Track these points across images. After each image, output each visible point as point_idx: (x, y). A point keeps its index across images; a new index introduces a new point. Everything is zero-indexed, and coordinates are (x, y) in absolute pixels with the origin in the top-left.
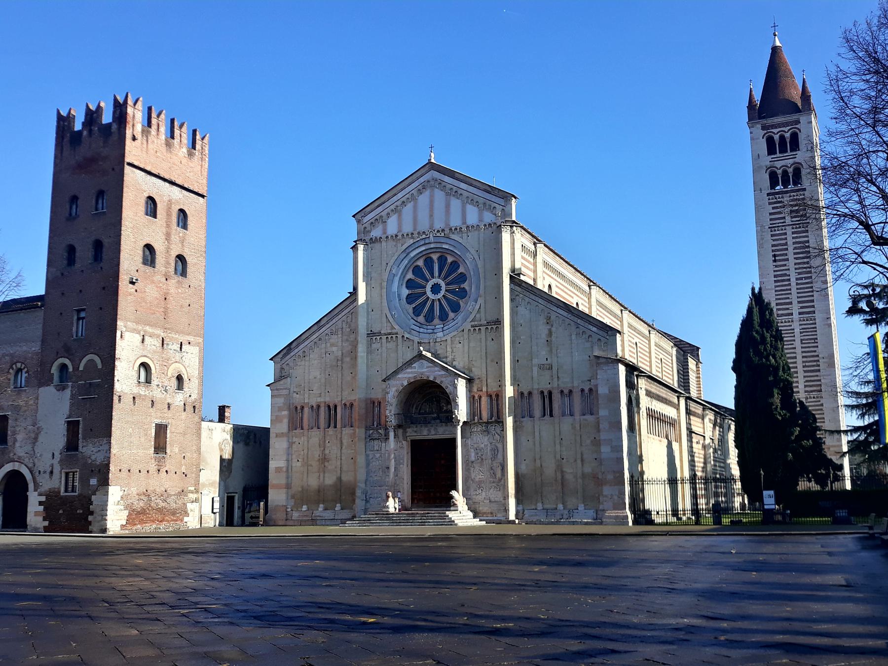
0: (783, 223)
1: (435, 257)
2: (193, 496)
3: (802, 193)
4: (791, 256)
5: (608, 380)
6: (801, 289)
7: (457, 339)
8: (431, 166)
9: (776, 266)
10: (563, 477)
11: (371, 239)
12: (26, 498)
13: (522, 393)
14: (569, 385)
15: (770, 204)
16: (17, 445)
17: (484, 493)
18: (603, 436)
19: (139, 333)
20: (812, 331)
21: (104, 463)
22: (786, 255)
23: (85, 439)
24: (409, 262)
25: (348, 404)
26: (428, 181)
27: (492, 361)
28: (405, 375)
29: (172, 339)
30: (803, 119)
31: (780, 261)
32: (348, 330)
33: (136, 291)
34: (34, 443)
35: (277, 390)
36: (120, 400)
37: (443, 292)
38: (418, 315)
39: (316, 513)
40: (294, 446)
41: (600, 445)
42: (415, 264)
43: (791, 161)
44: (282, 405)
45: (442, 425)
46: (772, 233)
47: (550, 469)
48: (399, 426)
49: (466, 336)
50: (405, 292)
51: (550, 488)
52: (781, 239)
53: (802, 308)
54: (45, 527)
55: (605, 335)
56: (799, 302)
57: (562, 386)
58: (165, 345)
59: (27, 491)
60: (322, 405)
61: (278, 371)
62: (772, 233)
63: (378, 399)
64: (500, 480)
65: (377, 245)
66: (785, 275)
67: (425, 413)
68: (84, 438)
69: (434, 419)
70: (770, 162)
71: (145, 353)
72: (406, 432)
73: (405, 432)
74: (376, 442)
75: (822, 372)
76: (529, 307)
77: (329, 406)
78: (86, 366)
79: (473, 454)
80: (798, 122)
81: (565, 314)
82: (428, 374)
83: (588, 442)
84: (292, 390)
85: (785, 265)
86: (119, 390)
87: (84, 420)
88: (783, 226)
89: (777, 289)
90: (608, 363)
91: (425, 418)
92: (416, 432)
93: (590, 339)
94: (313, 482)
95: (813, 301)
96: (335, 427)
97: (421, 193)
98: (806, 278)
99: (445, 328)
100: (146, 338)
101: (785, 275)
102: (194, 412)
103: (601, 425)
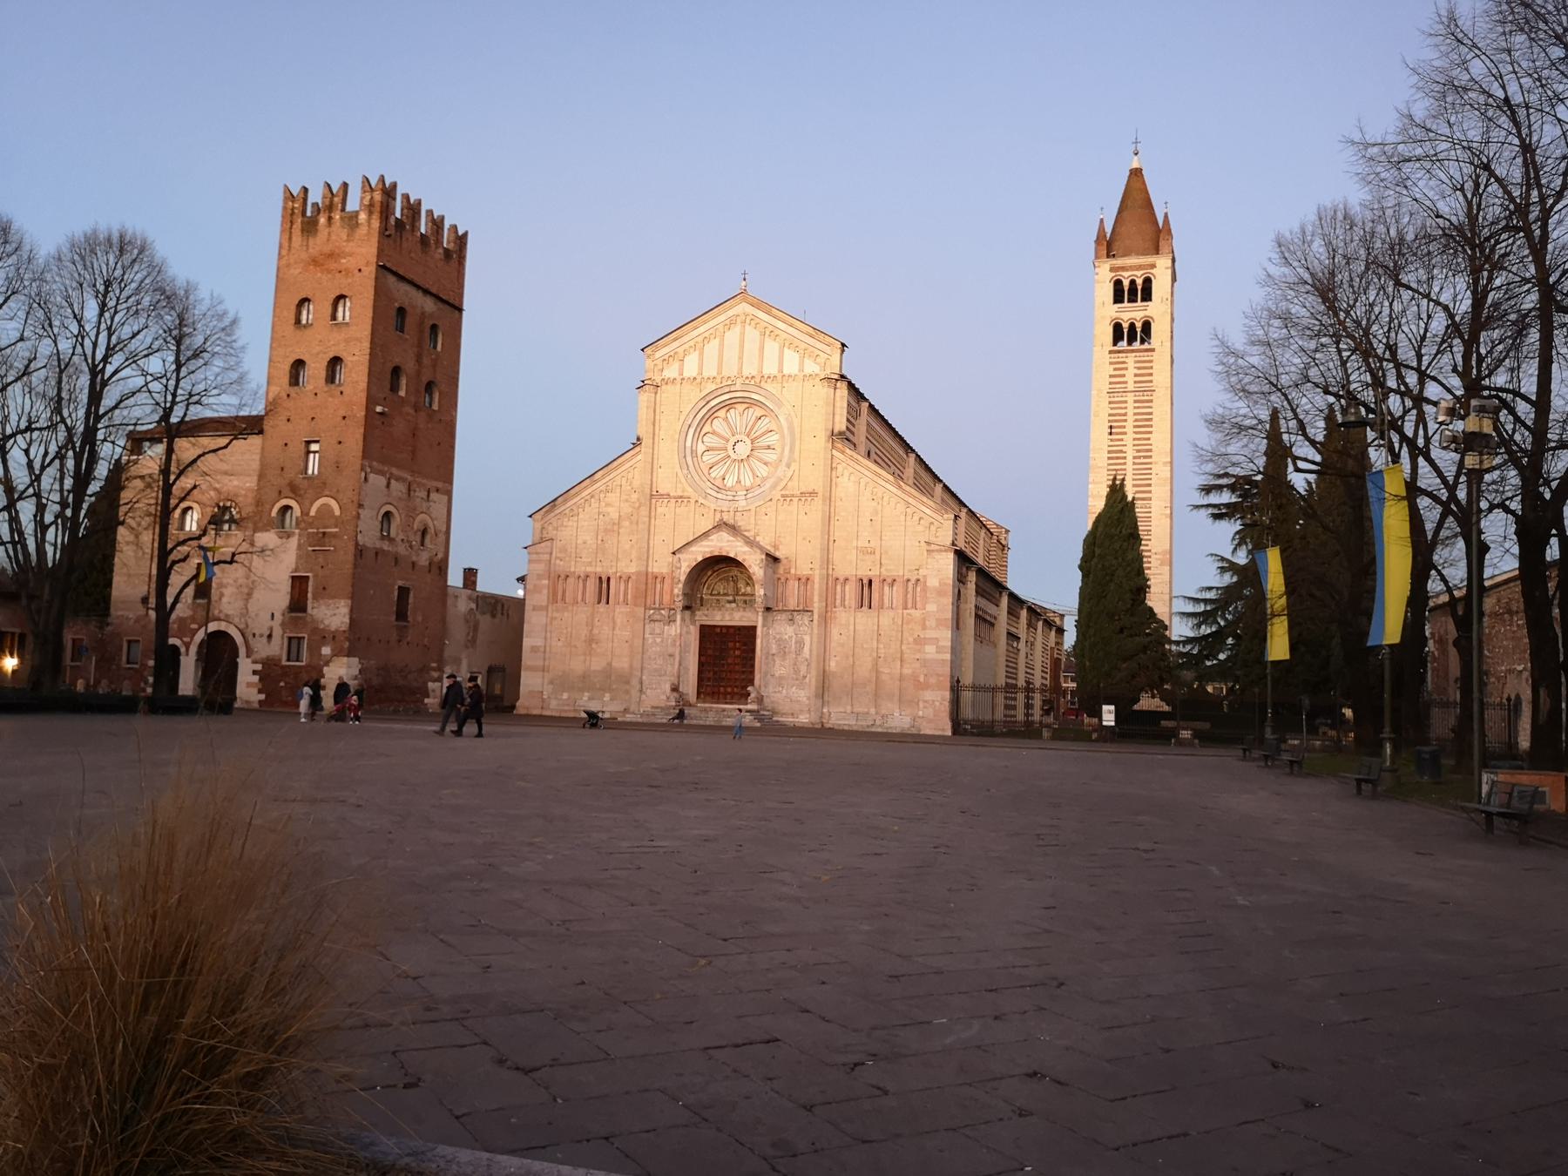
2: (435, 674)
3: (1150, 354)
7: (764, 510)
9: (1111, 440)
10: (877, 678)
12: (236, 665)
14: (896, 574)
15: (1111, 363)
16: (225, 600)
27: (804, 539)
29: (419, 484)
31: (1117, 434)
32: (629, 488)
34: (247, 600)
35: (537, 553)
40: (555, 623)
42: (716, 415)
43: (1141, 314)
44: (541, 572)
47: (864, 669)
48: (687, 608)
54: (260, 702)
55: (939, 518)
58: (412, 493)
59: (238, 657)
60: (592, 576)
65: (669, 387)
66: (1121, 451)
67: (719, 594)
68: (315, 598)
69: (730, 602)
71: (390, 500)
72: (695, 615)
73: (693, 614)
77: (600, 578)
78: (318, 511)
80: (1153, 266)
81: (894, 490)
82: (728, 549)
83: (911, 640)
86: (361, 543)
87: (314, 576)
90: (941, 551)
91: (718, 600)
93: (922, 521)
94: (577, 665)
95: (1150, 485)
96: (608, 603)
98: (1145, 457)
99: (748, 496)
100: (393, 481)
101: (1121, 451)
103: (927, 623)
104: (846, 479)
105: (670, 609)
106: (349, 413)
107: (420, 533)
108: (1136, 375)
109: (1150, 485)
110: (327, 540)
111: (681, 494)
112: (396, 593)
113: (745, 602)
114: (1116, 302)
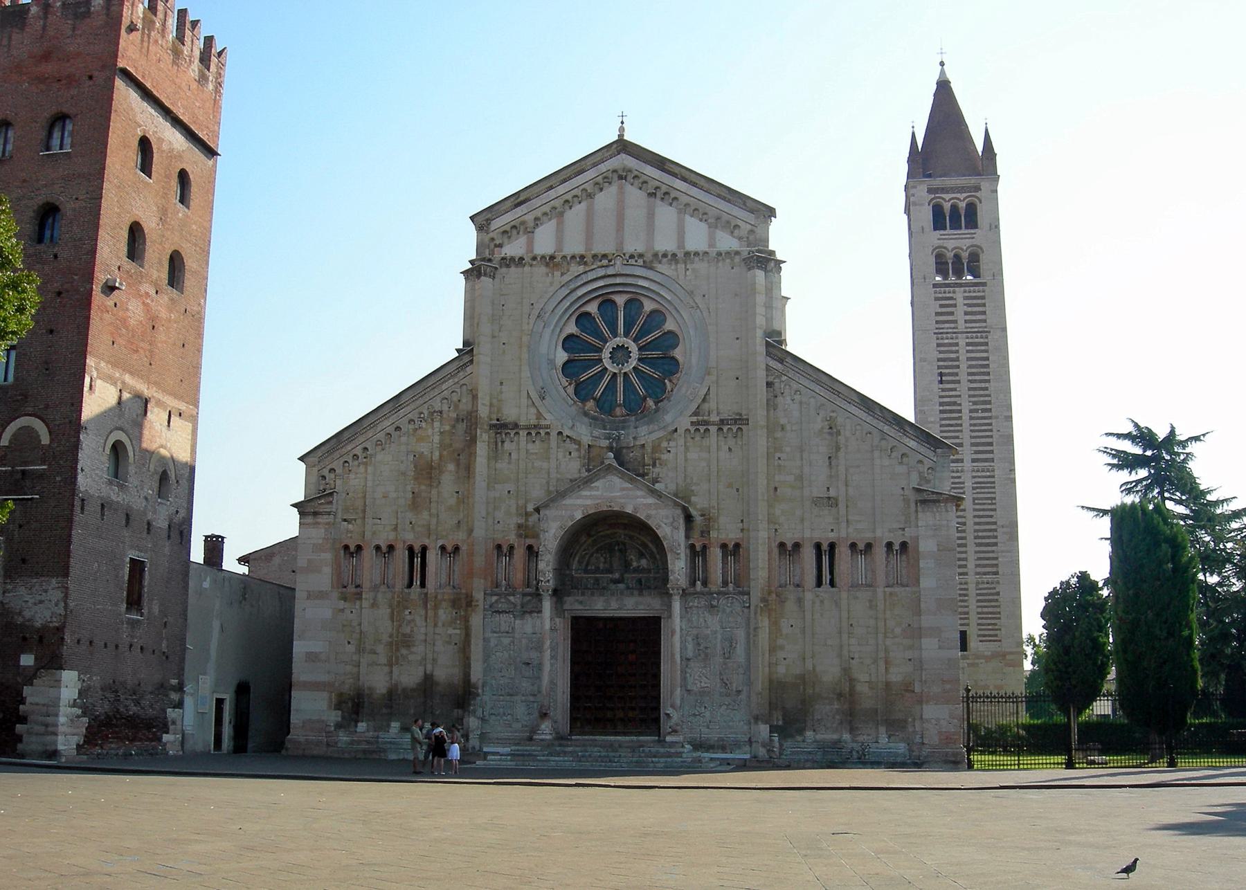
0: (954, 328)
1: (620, 300)
2: (174, 696)
3: (981, 288)
4: (963, 377)
5: (936, 529)
6: (975, 425)
8: (622, 146)
9: (943, 390)
11: (503, 259)
13: (782, 545)
15: (937, 299)
17: (707, 714)
18: (926, 621)
19: (114, 384)
20: (988, 488)
21: (51, 625)
22: (957, 374)
23: (10, 577)
24: (572, 304)
25: (449, 548)
26: (615, 171)
27: (730, 486)
28: (579, 502)
30: (985, 185)
31: (949, 382)
33: (115, 305)
36: (82, 509)
37: (633, 363)
38: (584, 401)
39: (384, 737)
41: (921, 638)
43: (968, 242)
44: (320, 541)
45: (632, 594)
46: (938, 341)
48: (556, 592)
49: (681, 441)
50: (562, 356)
51: (828, 707)
52: (952, 352)
53: (976, 452)
55: (931, 454)
56: (973, 445)
57: (854, 537)
61: (314, 479)
62: (938, 341)
63: (509, 540)
64: (739, 692)
66: (955, 404)
67: (597, 570)
69: (616, 582)
70: (939, 239)
71: (119, 424)
74: (504, 617)
75: (1000, 547)
76: (797, 397)
78: (15, 437)
79: (690, 647)
80: (978, 189)
82: (623, 501)
83: (898, 631)
84: (339, 515)
85: (955, 390)
86: (82, 489)
88: (955, 333)
89: (944, 422)
91: (597, 580)
92: (581, 603)
94: (378, 682)
95: (991, 444)
97: (601, 190)
98: (984, 410)
101: (955, 404)
102: (181, 543)
103: (923, 605)
104: (788, 398)
105: (524, 595)
106: (67, 286)
107: (157, 477)
108: (966, 313)
109: (991, 444)
110: (28, 483)
111: (533, 422)
112: (127, 570)
113: (640, 581)
114: (935, 229)
